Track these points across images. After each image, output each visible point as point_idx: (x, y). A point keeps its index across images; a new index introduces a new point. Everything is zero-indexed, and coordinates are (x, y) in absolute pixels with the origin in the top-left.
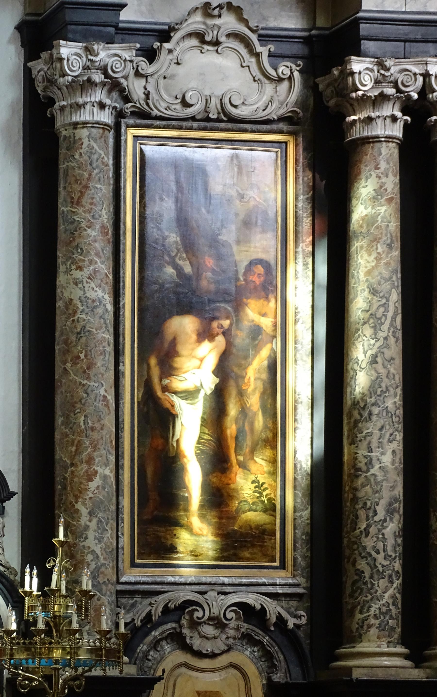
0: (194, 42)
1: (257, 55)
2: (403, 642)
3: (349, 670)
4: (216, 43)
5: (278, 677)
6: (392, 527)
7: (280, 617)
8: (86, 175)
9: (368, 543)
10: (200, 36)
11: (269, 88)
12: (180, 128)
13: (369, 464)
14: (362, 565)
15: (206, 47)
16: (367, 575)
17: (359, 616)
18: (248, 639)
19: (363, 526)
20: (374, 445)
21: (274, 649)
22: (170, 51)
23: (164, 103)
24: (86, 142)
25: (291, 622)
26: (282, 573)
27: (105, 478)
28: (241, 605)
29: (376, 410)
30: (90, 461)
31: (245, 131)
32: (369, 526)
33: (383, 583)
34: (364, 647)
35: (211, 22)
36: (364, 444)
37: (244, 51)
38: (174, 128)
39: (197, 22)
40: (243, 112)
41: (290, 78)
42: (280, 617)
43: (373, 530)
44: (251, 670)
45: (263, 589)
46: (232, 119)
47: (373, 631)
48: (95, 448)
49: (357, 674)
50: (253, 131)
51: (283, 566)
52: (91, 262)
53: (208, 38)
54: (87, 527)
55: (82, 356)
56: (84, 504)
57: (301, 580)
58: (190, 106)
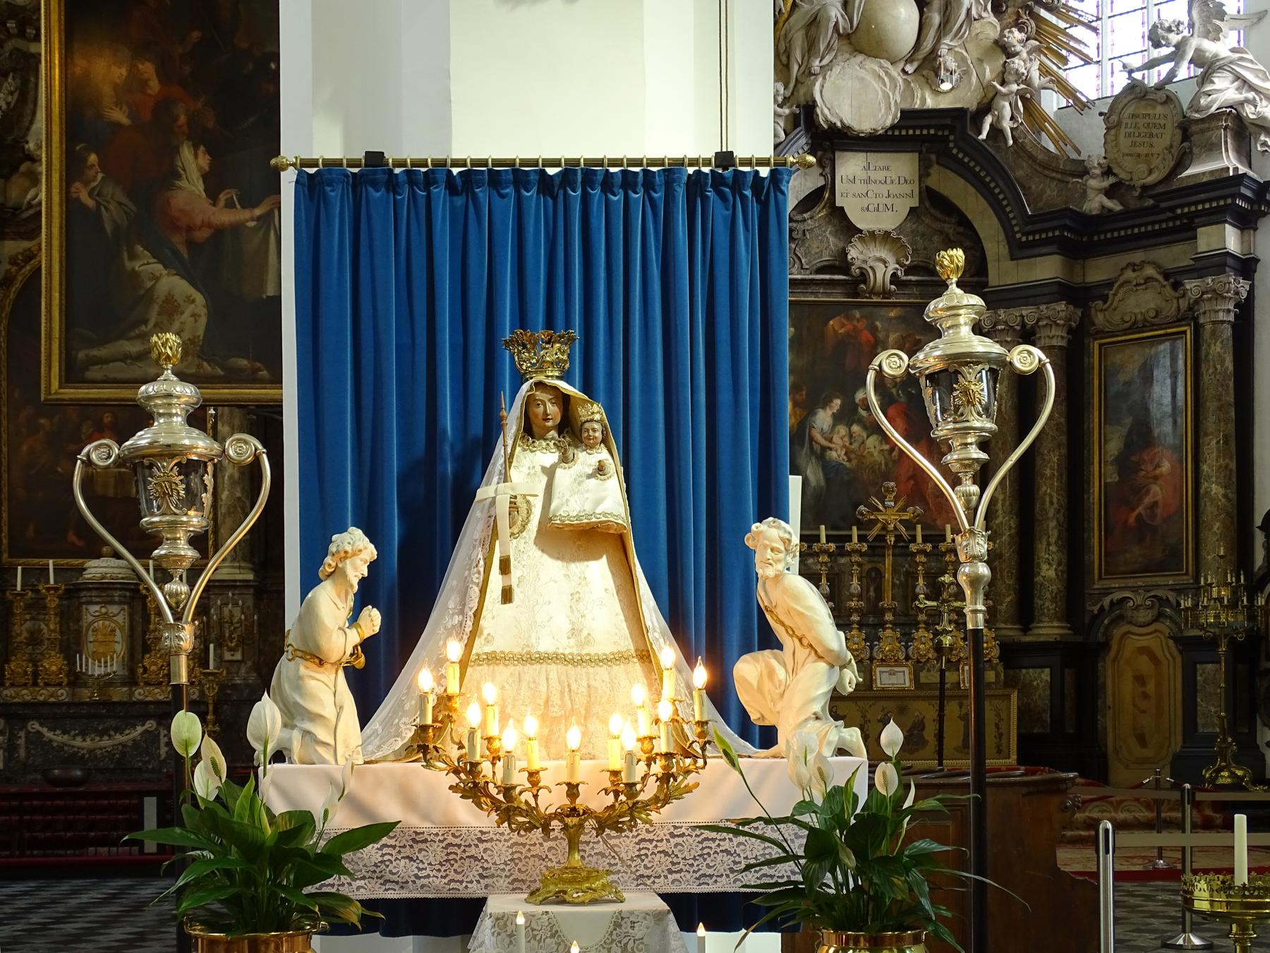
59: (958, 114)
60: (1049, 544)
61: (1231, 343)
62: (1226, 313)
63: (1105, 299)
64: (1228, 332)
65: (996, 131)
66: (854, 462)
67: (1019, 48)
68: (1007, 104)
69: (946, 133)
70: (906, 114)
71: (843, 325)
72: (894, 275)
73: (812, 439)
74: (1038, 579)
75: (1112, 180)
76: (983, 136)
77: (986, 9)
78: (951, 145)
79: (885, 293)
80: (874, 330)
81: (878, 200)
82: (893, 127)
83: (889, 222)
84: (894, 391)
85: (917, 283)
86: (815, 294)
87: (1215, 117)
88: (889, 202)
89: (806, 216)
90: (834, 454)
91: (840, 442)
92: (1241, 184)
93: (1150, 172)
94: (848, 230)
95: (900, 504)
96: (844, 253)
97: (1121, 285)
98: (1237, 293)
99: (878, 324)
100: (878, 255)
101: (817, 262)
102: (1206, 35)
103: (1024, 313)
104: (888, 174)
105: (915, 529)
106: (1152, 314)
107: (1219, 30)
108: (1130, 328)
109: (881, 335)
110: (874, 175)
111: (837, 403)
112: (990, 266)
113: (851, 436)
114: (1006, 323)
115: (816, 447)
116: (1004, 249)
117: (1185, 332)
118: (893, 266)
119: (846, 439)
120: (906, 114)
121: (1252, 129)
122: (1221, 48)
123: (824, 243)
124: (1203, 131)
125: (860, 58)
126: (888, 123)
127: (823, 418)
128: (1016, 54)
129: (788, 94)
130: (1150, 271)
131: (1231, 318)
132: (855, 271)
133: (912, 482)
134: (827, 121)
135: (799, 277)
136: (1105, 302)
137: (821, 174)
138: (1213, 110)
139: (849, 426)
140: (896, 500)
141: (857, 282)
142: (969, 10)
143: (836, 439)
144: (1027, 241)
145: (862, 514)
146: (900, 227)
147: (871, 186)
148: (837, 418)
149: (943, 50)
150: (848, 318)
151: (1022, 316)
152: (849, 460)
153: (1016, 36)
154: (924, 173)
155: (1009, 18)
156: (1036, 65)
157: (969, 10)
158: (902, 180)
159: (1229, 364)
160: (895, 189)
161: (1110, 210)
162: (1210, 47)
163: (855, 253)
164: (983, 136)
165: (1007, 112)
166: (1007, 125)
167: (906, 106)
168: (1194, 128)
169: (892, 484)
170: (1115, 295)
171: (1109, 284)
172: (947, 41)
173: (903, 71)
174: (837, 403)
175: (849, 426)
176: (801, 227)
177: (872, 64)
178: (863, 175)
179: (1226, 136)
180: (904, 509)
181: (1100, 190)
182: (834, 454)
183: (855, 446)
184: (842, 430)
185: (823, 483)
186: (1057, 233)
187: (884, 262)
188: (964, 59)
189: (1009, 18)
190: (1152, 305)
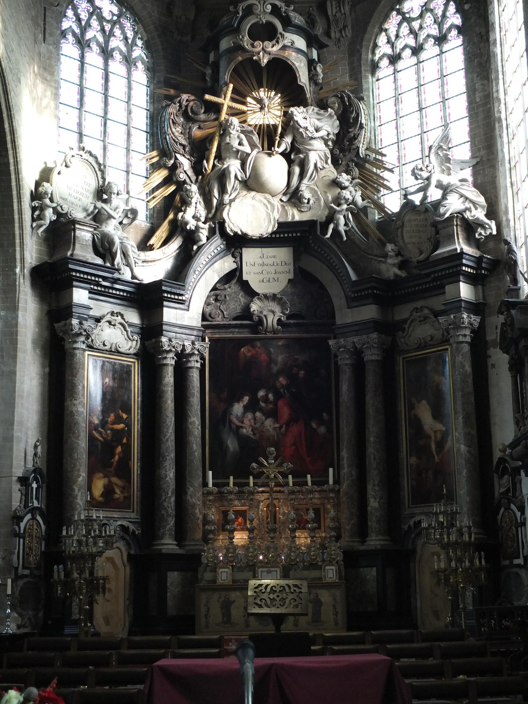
0: (107, 323)
1: (127, 331)
2: (176, 540)
3: (161, 549)
4: (114, 325)
5: (132, 552)
6: (173, 499)
7: (133, 530)
8: (78, 366)
9: (166, 504)
10: (110, 322)
11: (130, 343)
12: (103, 353)
13: (166, 476)
14: (163, 512)
15: (112, 326)
16: (165, 515)
17: (162, 531)
18: (123, 538)
19: (164, 498)
20: (167, 470)
21: (131, 542)
22: (100, 326)
23: (98, 344)
24: (78, 355)
25: (137, 532)
26: (133, 514)
27: (83, 477)
28: (121, 526)
29: (168, 458)
30: (79, 470)
31: (123, 357)
32: (166, 498)
33: (170, 519)
34: (165, 541)
35: (113, 318)
36: (164, 469)
37: (123, 329)
38: (101, 353)
39: (108, 317)
40: (121, 350)
41: (137, 341)
42: (133, 530)
43: (167, 500)
44: (123, 549)
45: (128, 520)
46: (119, 352)
47: (167, 536)
48: (81, 466)
49: (164, 551)
50: (125, 357)
51: (133, 511)
52: (80, 398)
53: (112, 323)
54: (77, 495)
55: (76, 432)
56: (76, 486)
57: (139, 517)
58: (106, 346)
59: (312, 223)
60: (374, 485)
61: (469, 355)
62: (465, 336)
63: (403, 330)
64: (466, 348)
65: (336, 231)
66: (257, 435)
67: (347, 184)
68: (342, 217)
69: (308, 235)
70: (281, 225)
71: (249, 351)
72: (279, 320)
73: (230, 422)
74: (369, 508)
75: (400, 258)
76: (328, 235)
77: (327, 163)
78: (311, 242)
79: (274, 331)
80: (269, 354)
81: (269, 276)
82: (273, 233)
83: (276, 288)
84: (282, 390)
85: (295, 325)
86: (233, 333)
87: (451, 218)
88: (276, 277)
89: (226, 286)
90: (244, 431)
91: (248, 423)
92: (462, 258)
93: (421, 253)
94: (251, 293)
95: (277, 463)
96: (247, 308)
97: (412, 322)
98: (472, 324)
99: (272, 350)
100: (270, 308)
101: (234, 314)
102: (443, 171)
103: (355, 340)
104: (273, 259)
105: (287, 477)
106: (429, 339)
107: (449, 169)
108: (418, 348)
109: (273, 356)
110: (266, 261)
111: (246, 399)
112: (336, 312)
113: (255, 419)
114: (345, 347)
115: (234, 427)
116: (344, 302)
117: (447, 349)
118: (278, 314)
119: (252, 421)
120: (281, 225)
121: (473, 225)
122: (453, 179)
123: (235, 301)
124: (444, 228)
125: (253, 193)
126: (270, 230)
127: (238, 408)
128: (345, 188)
129: (210, 216)
130: (426, 311)
131: (468, 339)
132: (256, 318)
133: (294, 447)
134: (231, 230)
135: (222, 323)
136: (404, 333)
137: (234, 262)
138: (447, 215)
139: (254, 413)
140: (276, 459)
141: (257, 324)
142: (316, 165)
143: (246, 421)
144: (354, 297)
145: (253, 468)
146: (283, 290)
147: (264, 268)
148: (246, 408)
149: (303, 187)
150: (253, 346)
151: (354, 342)
152: (254, 434)
153: (344, 178)
154: (297, 257)
155: (342, 168)
156: (359, 193)
157: (316, 165)
158: (283, 264)
159: (468, 368)
160: (280, 269)
161: (401, 277)
162: (445, 180)
163: (255, 307)
164: (328, 235)
165: (342, 221)
166: (342, 228)
167: (281, 220)
168: (440, 226)
169: (273, 449)
170: (409, 328)
171: (405, 321)
172: (305, 181)
173: (281, 200)
174: (246, 399)
175: (254, 413)
176: (223, 293)
177: (259, 196)
178: (260, 261)
179: (457, 230)
180: (280, 465)
181: (394, 265)
182: (244, 431)
183: (258, 425)
184: (250, 416)
185: (237, 449)
186: (370, 291)
187: (273, 312)
188: (316, 192)
189: (342, 168)
190: (429, 334)
